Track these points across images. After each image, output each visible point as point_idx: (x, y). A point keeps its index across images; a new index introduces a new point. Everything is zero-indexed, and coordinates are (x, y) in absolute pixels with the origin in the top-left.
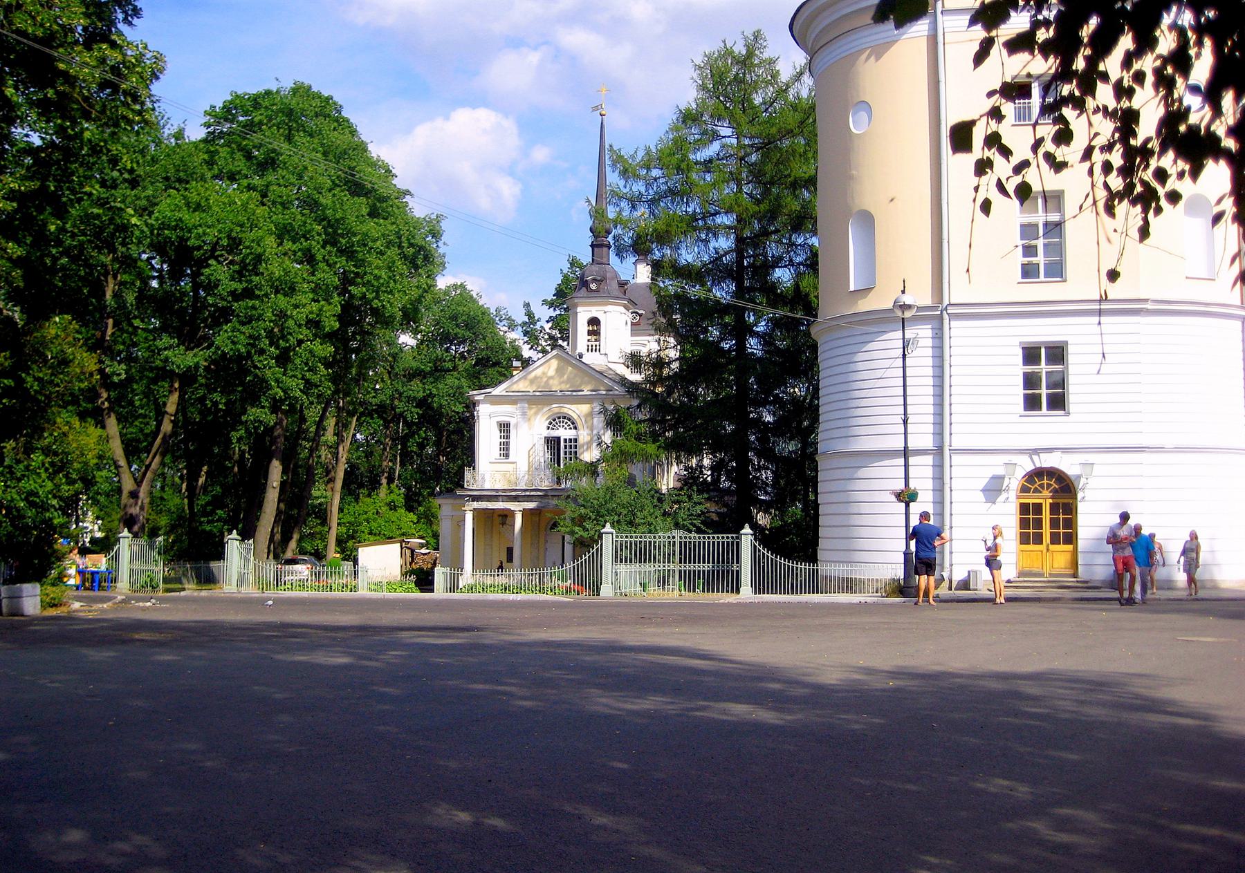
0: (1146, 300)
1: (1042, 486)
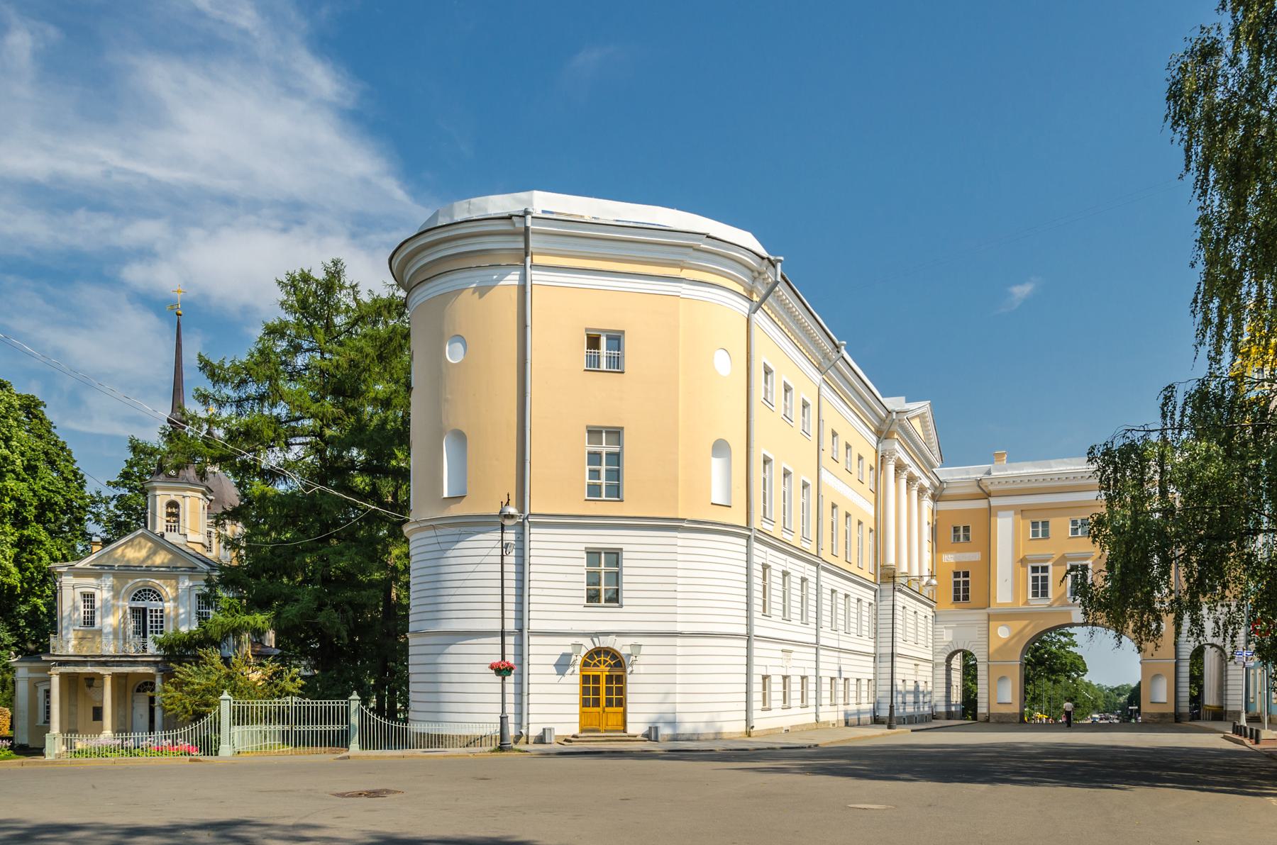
0: (683, 520)
1: (599, 662)
